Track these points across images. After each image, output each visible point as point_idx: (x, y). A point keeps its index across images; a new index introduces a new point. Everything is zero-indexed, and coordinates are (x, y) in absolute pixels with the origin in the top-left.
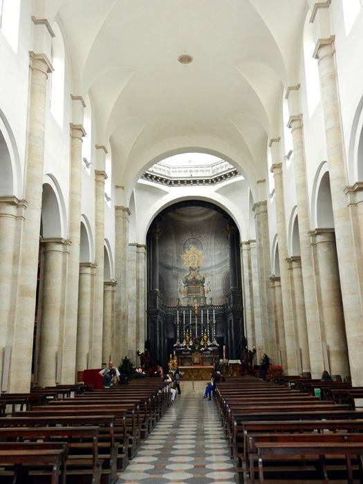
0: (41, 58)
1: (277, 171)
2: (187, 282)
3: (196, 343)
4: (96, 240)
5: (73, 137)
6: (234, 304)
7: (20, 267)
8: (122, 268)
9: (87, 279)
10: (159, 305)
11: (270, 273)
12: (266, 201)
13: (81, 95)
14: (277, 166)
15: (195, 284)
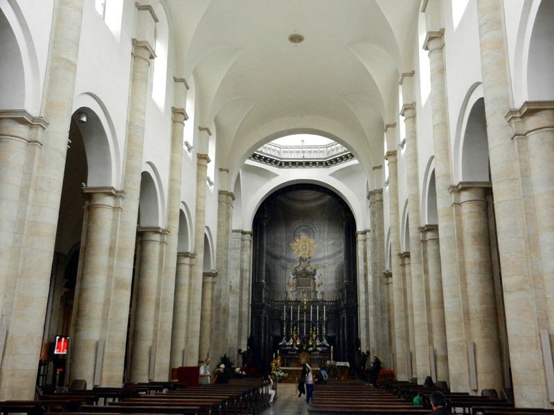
0: (144, 45)
1: (391, 158)
2: (297, 274)
3: (304, 342)
4: (196, 227)
5: (174, 121)
6: (348, 298)
7: (115, 258)
8: (224, 258)
9: (185, 269)
10: (265, 299)
11: (384, 268)
12: (382, 190)
13: (184, 78)
14: (392, 154)
15: (306, 276)
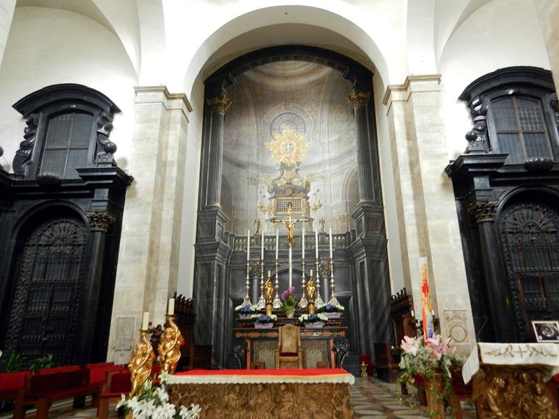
2: (276, 191)
3: (290, 304)
6: (367, 230)
10: (221, 235)
15: (291, 194)
